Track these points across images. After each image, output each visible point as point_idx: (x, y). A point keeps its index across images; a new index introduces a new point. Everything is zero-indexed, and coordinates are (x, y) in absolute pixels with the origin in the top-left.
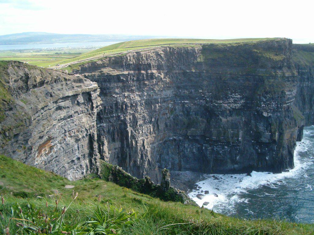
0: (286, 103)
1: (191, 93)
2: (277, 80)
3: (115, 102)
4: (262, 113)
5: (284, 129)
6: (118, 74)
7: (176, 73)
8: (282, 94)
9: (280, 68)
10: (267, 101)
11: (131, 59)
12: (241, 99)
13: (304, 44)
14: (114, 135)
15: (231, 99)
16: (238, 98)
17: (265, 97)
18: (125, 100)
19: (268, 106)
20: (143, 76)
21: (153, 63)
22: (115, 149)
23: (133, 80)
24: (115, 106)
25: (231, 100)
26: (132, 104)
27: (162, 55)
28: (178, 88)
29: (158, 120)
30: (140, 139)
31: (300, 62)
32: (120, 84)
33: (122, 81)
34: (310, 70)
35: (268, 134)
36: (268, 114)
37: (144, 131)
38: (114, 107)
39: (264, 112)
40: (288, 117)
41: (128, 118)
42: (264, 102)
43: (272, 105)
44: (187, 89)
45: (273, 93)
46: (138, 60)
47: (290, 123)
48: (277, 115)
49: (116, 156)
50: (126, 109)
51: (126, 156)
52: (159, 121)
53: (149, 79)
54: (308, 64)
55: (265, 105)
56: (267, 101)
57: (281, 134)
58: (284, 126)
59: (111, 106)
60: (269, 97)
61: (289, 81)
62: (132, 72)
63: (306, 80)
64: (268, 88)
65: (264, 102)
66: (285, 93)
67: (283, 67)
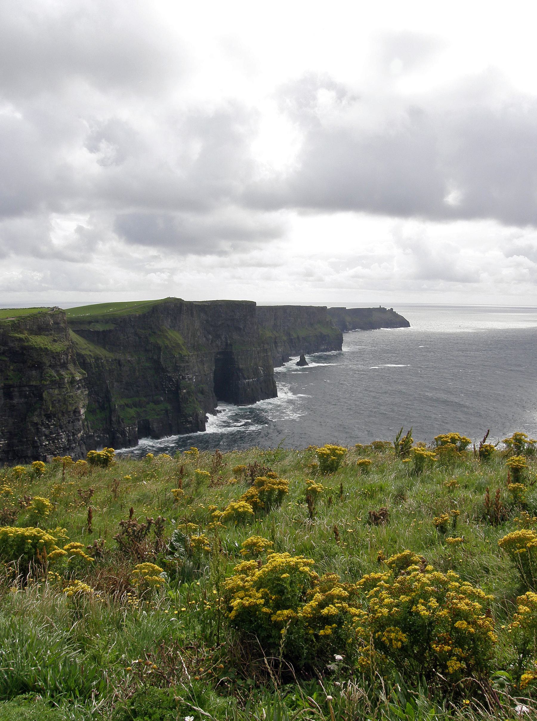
2: (64, 390)
8: (75, 416)
10: (51, 433)
13: (512, 329)
17: (48, 427)
19: (53, 442)
39: (48, 455)
40: (83, 457)
42: (46, 436)
43: (61, 439)
45: (60, 415)
55: (49, 443)
60: (53, 424)
65: (46, 436)
66: (79, 412)
67: (67, 363)
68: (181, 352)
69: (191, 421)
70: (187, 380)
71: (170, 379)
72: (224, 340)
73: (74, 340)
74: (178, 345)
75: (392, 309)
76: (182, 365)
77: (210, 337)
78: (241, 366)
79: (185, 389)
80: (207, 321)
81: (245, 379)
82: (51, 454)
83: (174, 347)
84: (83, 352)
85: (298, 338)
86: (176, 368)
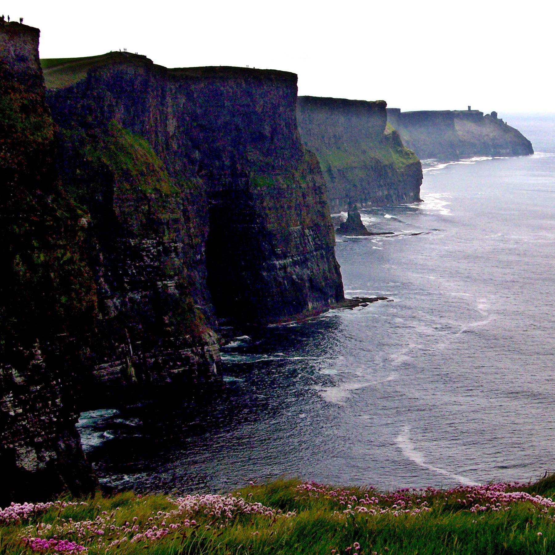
4: (14, 455)
36: (41, 459)
39: (21, 446)
42: (18, 390)
56: (30, 381)
65: (18, 390)
68: (158, 187)
69: (188, 358)
70: (173, 255)
71: (136, 253)
72: (227, 163)
75: (494, 114)
76: (165, 216)
77: (197, 155)
78: (270, 227)
79: (171, 278)
80: (194, 117)
81: (279, 257)
82: (27, 444)
83: (142, 174)
85: (329, 170)
86: (153, 226)
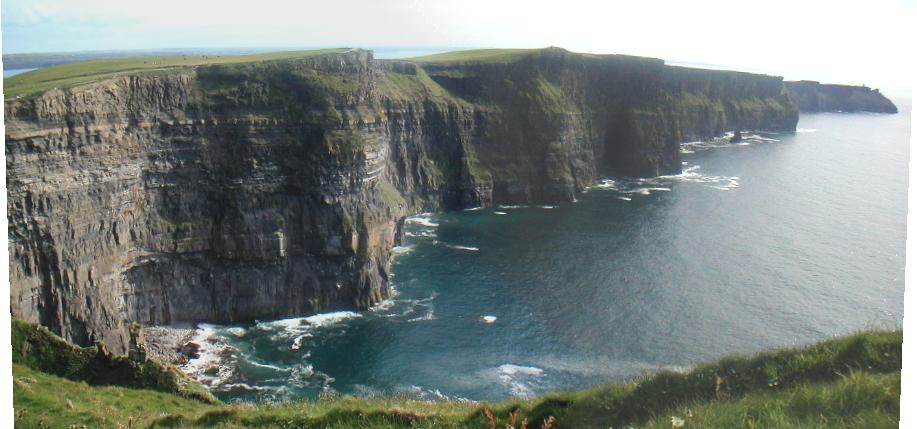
0: (369, 176)
1: (179, 165)
3: (24, 195)
4: (323, 197)
5: (367, 225)
6: (28, 135)
7: (146, 129)
9: (353, 107)
11: (53, 104)
12: (278, 173)
14: (28, 261)
15: (260, 173)
16: (273, 171)
18: (46, 188)
20: (79, 138)
21: (98, 110)
22: (32, 290)
23: (60, 147)
24: (26, 202)
25: (260, 177)
26: (60, 198)
27: (116, 94)
28: (153, 158)
29: (115, 224)
30: (82, 269)
31: (390, 93)
32: (35, 157)
33: (38, 149)
34: (410, 108)
35: (336, 240)
37: (88, 251)
38: (24, 204)
41: (53, 225)
44: (170, 160)
46: (68, 104)
47: (379, 215)
48: (352, 201)
49: (36, 304)
50: (50, 208)
51: (57, 302)
52: (118, 227)
53: (93, 142)
54: (406, 98)
57: (363, 237)
58: (366, 220)
59: (17, 204)
61: (370, 132)
62: (58, 131)
63: (403, 129)
64: (331, 148)
65: (324, 176)
73: (428, 86)
74: (551, 101)
84: (435, 100)
